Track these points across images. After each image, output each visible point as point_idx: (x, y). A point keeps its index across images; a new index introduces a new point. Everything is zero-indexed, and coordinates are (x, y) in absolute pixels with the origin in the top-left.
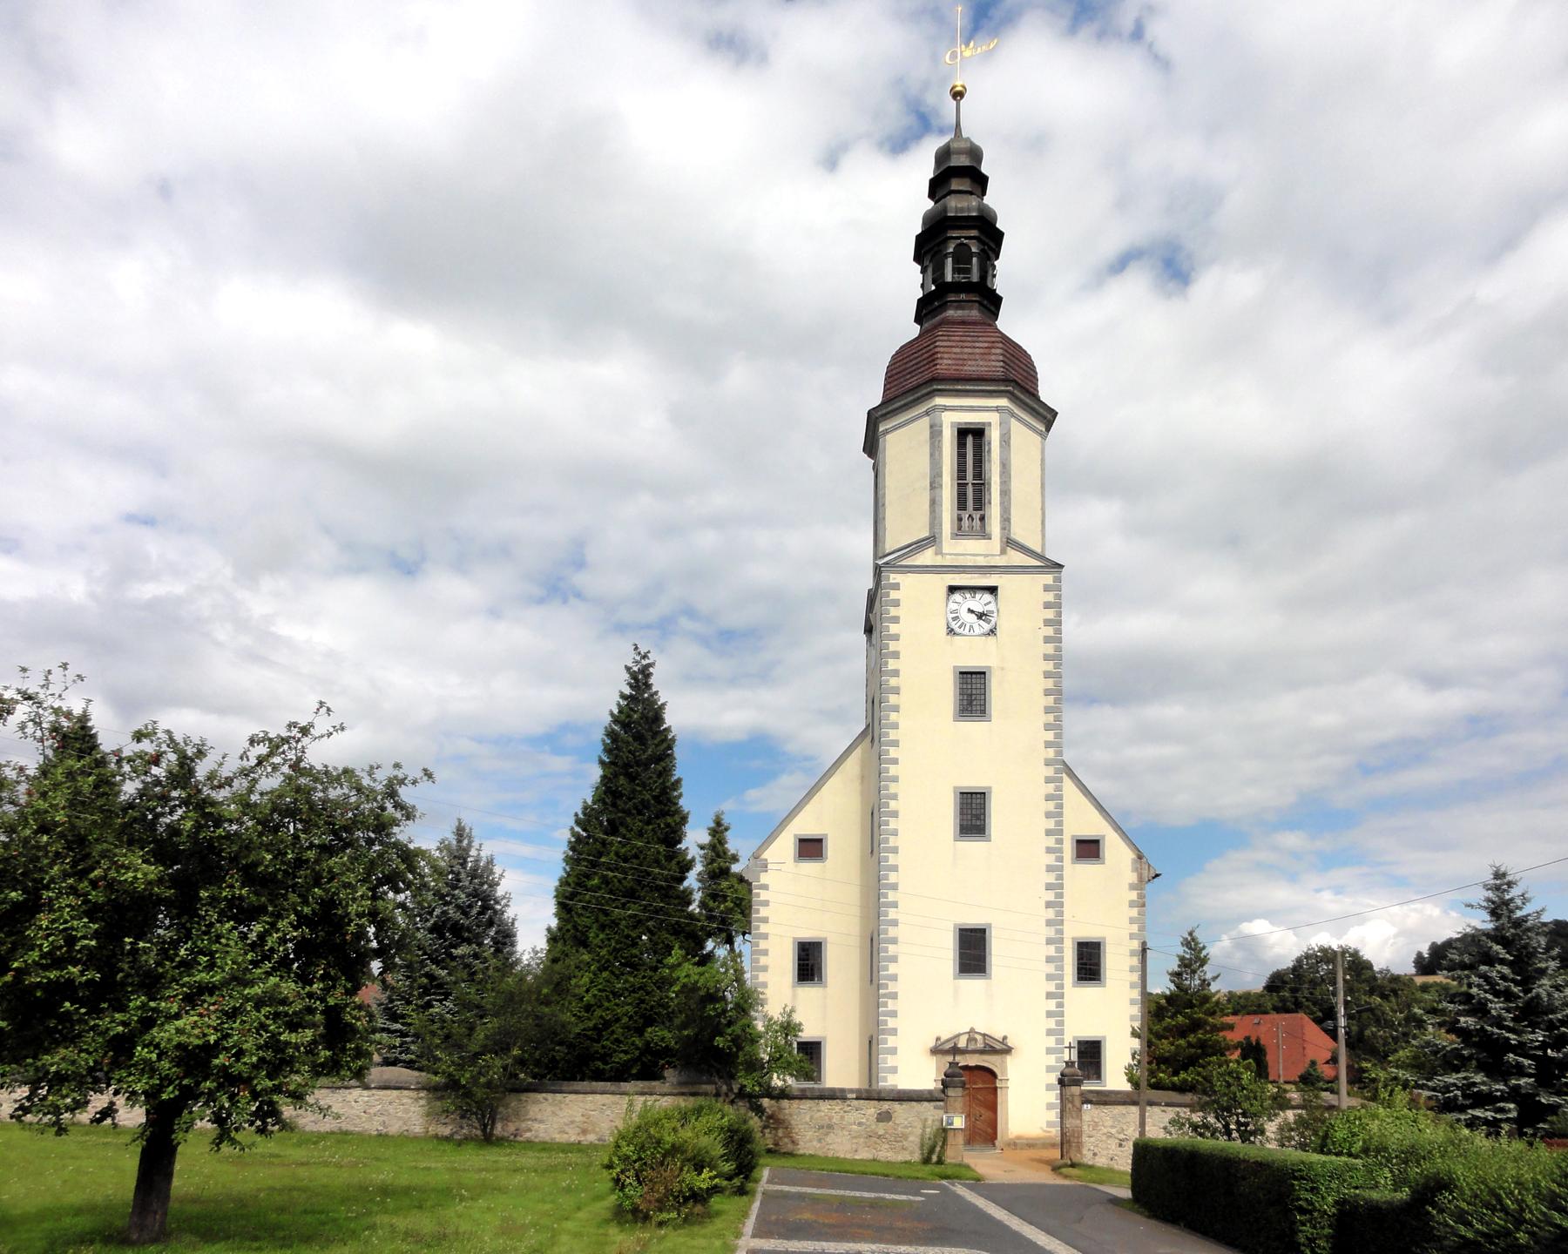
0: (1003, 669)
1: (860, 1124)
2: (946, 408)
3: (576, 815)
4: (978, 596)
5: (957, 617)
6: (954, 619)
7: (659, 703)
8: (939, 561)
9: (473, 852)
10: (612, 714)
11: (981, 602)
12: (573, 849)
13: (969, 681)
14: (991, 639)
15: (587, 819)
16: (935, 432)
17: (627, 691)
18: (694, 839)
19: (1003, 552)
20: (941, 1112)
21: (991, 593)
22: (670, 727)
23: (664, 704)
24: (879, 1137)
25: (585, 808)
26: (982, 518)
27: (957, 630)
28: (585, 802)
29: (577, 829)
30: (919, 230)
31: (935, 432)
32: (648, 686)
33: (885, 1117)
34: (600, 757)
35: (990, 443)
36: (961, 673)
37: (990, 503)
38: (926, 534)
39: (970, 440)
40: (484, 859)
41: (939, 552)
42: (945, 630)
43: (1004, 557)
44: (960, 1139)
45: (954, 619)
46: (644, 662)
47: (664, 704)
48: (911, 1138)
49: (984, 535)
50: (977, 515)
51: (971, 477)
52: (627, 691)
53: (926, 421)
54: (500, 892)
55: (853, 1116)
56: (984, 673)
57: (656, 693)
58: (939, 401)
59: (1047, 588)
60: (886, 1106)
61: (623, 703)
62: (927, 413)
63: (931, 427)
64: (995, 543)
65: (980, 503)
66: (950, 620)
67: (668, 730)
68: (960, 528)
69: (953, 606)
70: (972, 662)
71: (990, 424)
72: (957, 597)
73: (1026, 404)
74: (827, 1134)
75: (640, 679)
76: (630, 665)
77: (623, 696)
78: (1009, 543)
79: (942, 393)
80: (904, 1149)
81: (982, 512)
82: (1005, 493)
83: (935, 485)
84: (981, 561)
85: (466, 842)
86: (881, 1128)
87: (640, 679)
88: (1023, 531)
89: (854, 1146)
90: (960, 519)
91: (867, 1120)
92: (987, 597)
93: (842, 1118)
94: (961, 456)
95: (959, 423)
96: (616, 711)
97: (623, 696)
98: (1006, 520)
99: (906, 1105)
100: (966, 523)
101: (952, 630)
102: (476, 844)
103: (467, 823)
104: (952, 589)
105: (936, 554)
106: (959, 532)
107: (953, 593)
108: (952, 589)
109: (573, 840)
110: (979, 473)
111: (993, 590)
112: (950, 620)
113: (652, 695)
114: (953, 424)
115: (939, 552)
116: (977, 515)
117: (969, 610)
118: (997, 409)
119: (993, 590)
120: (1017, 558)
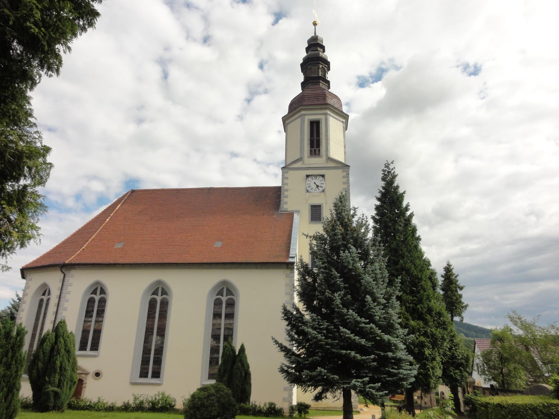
4: (318, 177)
5: (310, 186)
6: (309, 187)
11: (318, 181)
13: (315, 208)
16: (303, 122)
21: (323, 177)
26: (319, 151)
27: (309, 190)
31: (303, 122)
36: (311, 206)
41: (303, 163)
42: (305, 191)
45: (309, 187)
50: (317, 149)
51: (315, 137)
53: (300, 119)
56: (320, 206)
58: (303, 112)
62: (300, 116)
64: (324, 158)
65: (318, 145)
66: (307, 187)
69: (309, 182)
70: (316, 202)
72: (310, 179)
73: (323, 108)
79: (304, 110)
83: (302, 141)
92: (321, 178)
95: (311, 119)
101: (308, 191)
104: (308, 176)
107: (308, 177)
108: (308, 176)
111: (323, 176)
112: (307, 187)
114: (308, 119)
115: (303, 163)
117: (315, 183)
119: (323, 176)
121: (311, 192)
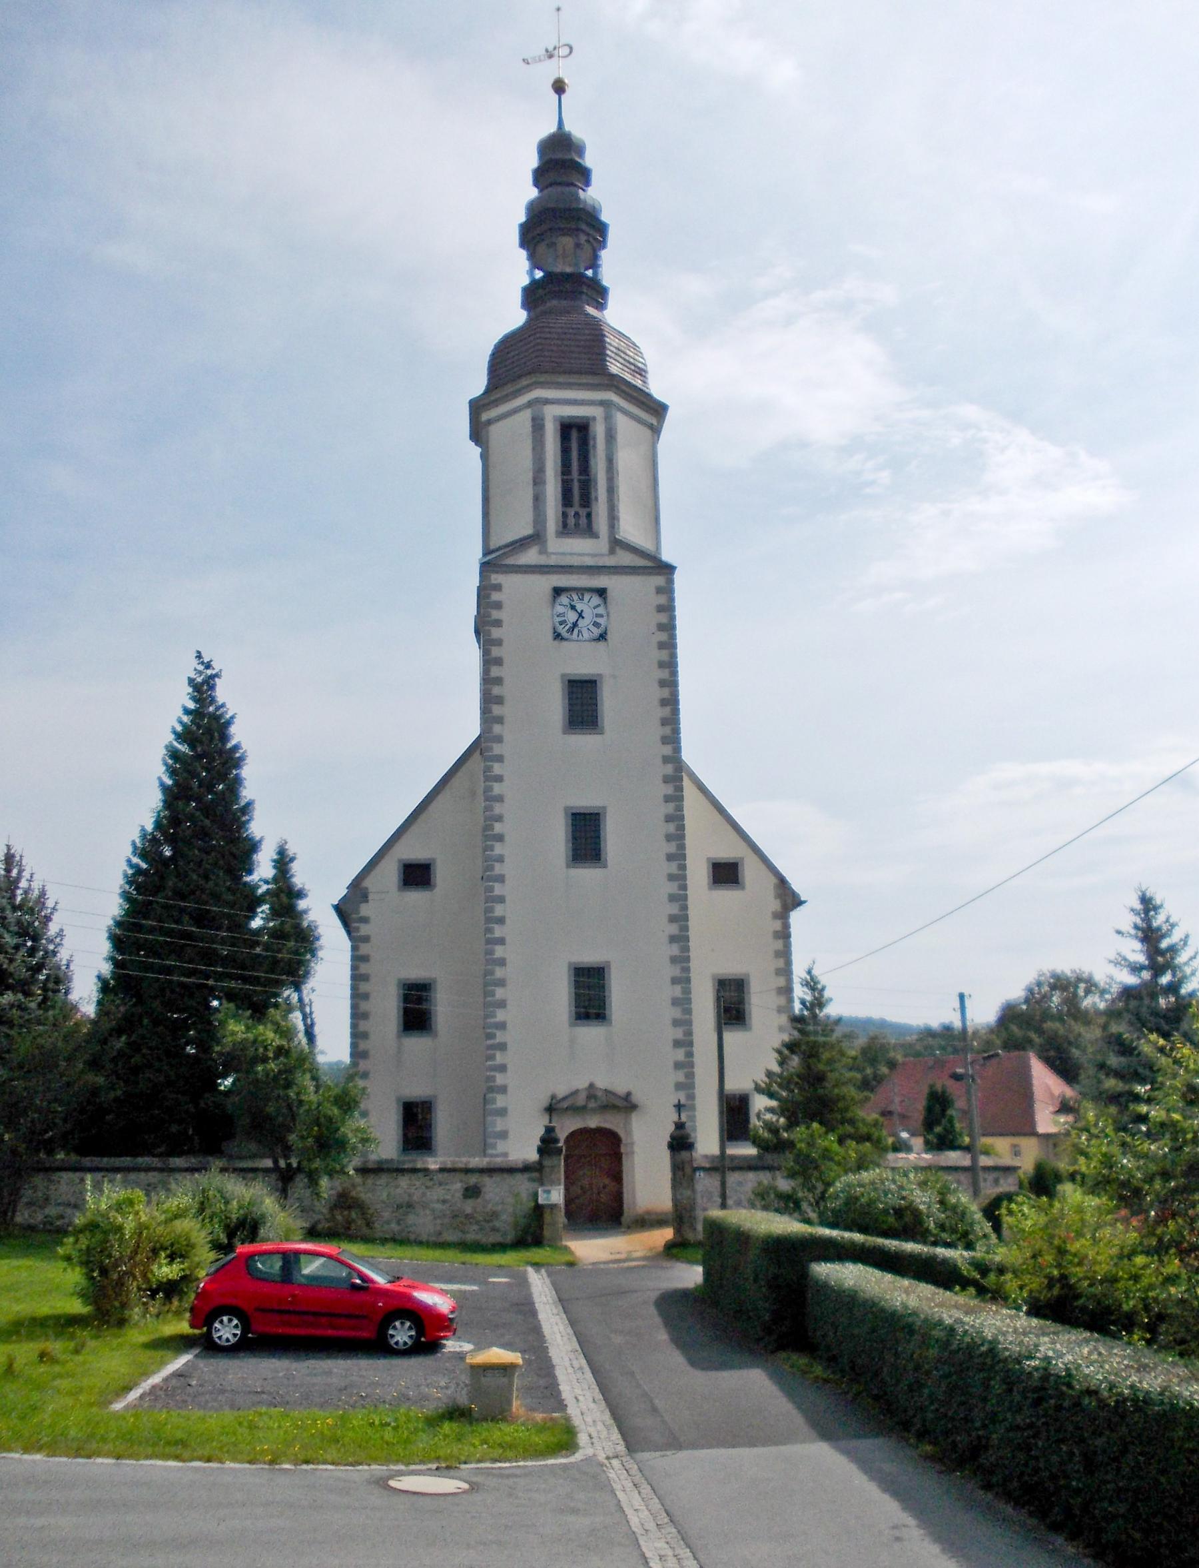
0: (614, 677)
1: (444, 1202)
2: (547, 402)
3: (134, 843)
7: (228, 716)
8: (542, 560)
9: (23, 884)
10: (174, 732)
11: (588, 606)
12: (130, 883)
14: (602, 644)
15: (148, 849)
17: (191, 705)
18: (263, 870)
19: (612, 551)
20: (535, 1185)
22: (239, 742)
23: (232, 717)
24: (467, 1216)
25: (144, 834)
26: (589, 515)
28: (143, 829)
29: (136, 860)
30: (522, 218)
31: (538, 426)
32: (213, 700)
33: (472, 1192)
34: (160, 779)
35: (594, 438)
37: (596, 499)
38: (529, 531)
39: (574, 435)
40: (36, 893)
41: (543, 551)
42: (550, 635)
43: (612, 557)
44: (561, 1219)
46: (209, 672)
47: (232, 717)
48: (504, 1217)
49: (589, 530)
50: (583, 512)
52: (191, 705)
54: (53, 928)
55: (437, 1193)
57: (223, 706)
59: (659, 590)
60: (473, 1179)
61: (186, 719)
63: (533, 419)
64: (602, 544)
65: (587, 500)
67: (236, 748)
68: (565, 525)
69: (560, 609)
71: (594, 418)
74: (406, 1214)
75: (203, 689)
76: (193, 675)
77: (187, 711)
78: (617, 544)
80: (494, 1229)
81: (588, 510)
82: (611, 490)
83: (538, 480)
84: (589, 561)
85: (14, 873)
86: (469, 1206)
87: (203, 689)
88: (631, 529)
89: (438, 1228)
90: (565, 515)
91: (453, 1196)
93: (424, 1194)
94: (565, 451)
95: (562, 417)
96: (179, 728)
97: (187, 711)
98: (613, 518)
99: (497, 1178)
100: (571, 521)
102: (26, 874)
103: (17, 850)
105: (541, 553)
106: (565, 530)
108: (558, 591)
109: (130, 872)
110: (585, 468)
113: (218, 708)
114: (555, 418)
115: (543, 551)
116: (583, 512)
118: (602, 403)
119: (602, 592)
120: (625, 558)
121: (566, 640)
